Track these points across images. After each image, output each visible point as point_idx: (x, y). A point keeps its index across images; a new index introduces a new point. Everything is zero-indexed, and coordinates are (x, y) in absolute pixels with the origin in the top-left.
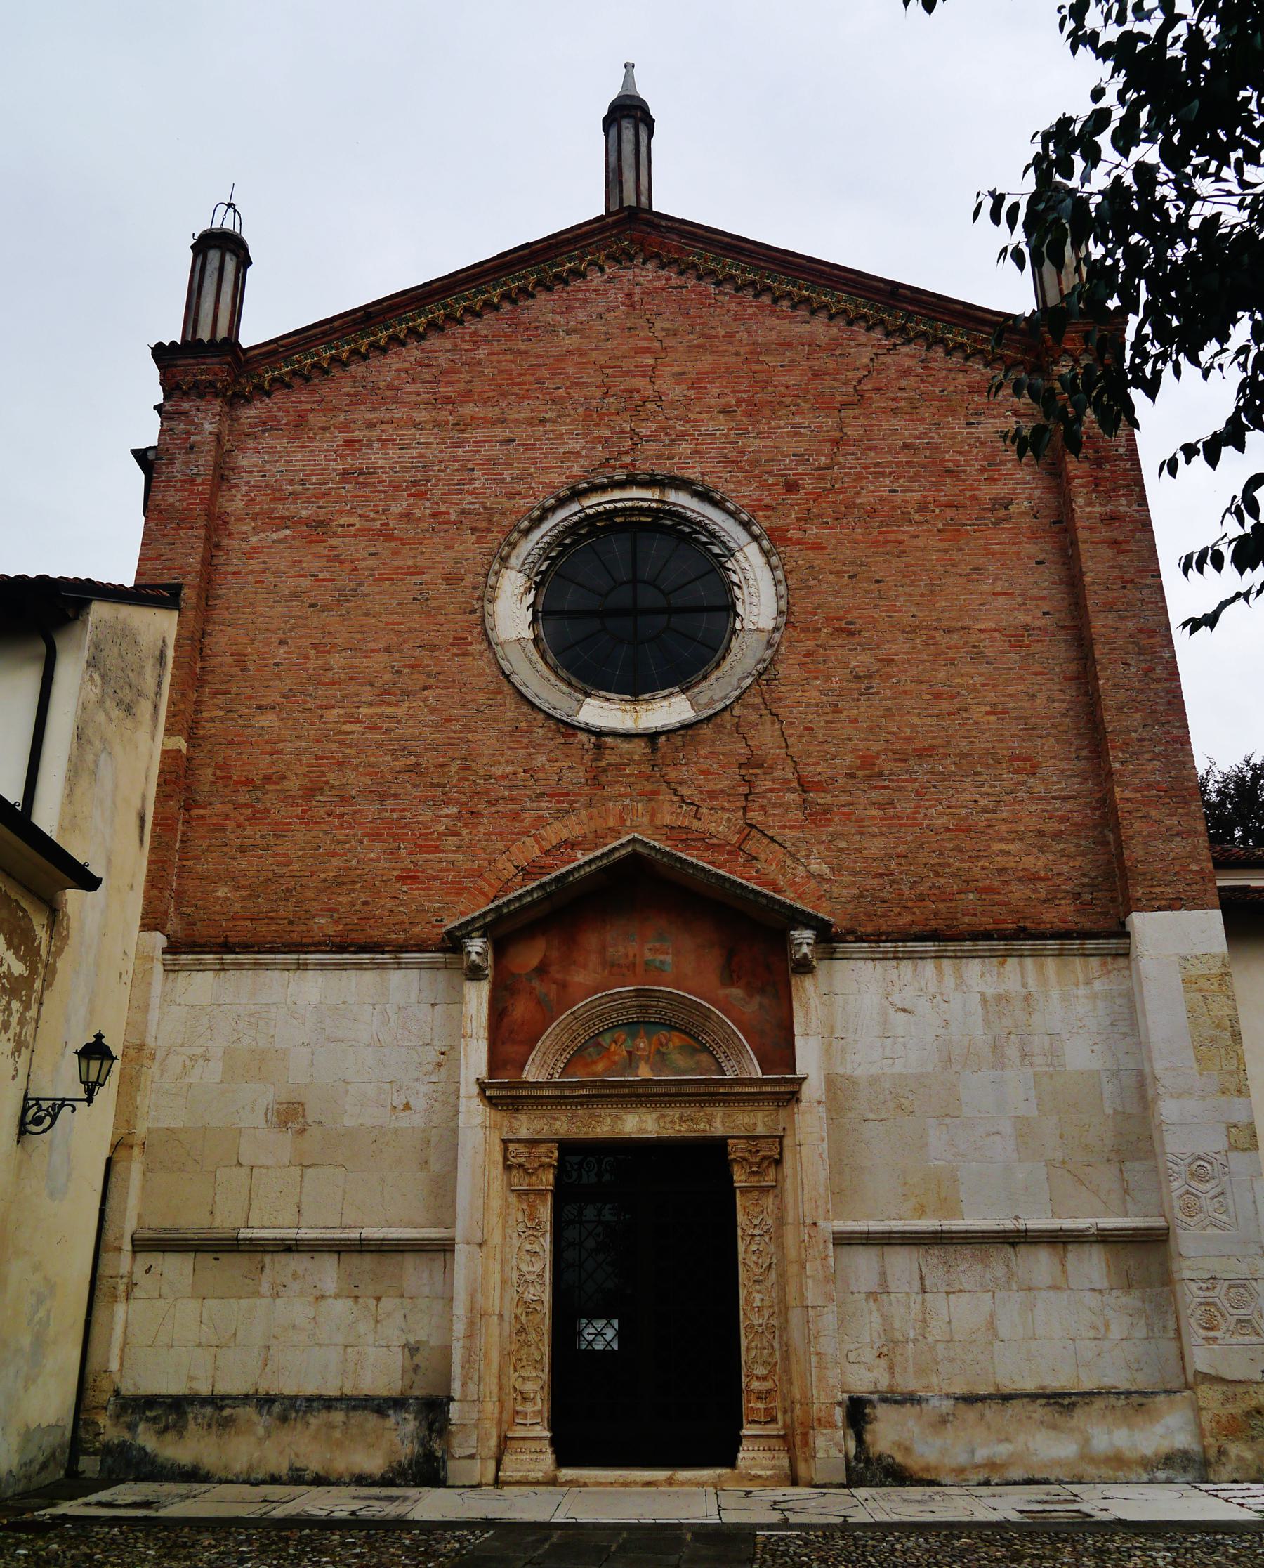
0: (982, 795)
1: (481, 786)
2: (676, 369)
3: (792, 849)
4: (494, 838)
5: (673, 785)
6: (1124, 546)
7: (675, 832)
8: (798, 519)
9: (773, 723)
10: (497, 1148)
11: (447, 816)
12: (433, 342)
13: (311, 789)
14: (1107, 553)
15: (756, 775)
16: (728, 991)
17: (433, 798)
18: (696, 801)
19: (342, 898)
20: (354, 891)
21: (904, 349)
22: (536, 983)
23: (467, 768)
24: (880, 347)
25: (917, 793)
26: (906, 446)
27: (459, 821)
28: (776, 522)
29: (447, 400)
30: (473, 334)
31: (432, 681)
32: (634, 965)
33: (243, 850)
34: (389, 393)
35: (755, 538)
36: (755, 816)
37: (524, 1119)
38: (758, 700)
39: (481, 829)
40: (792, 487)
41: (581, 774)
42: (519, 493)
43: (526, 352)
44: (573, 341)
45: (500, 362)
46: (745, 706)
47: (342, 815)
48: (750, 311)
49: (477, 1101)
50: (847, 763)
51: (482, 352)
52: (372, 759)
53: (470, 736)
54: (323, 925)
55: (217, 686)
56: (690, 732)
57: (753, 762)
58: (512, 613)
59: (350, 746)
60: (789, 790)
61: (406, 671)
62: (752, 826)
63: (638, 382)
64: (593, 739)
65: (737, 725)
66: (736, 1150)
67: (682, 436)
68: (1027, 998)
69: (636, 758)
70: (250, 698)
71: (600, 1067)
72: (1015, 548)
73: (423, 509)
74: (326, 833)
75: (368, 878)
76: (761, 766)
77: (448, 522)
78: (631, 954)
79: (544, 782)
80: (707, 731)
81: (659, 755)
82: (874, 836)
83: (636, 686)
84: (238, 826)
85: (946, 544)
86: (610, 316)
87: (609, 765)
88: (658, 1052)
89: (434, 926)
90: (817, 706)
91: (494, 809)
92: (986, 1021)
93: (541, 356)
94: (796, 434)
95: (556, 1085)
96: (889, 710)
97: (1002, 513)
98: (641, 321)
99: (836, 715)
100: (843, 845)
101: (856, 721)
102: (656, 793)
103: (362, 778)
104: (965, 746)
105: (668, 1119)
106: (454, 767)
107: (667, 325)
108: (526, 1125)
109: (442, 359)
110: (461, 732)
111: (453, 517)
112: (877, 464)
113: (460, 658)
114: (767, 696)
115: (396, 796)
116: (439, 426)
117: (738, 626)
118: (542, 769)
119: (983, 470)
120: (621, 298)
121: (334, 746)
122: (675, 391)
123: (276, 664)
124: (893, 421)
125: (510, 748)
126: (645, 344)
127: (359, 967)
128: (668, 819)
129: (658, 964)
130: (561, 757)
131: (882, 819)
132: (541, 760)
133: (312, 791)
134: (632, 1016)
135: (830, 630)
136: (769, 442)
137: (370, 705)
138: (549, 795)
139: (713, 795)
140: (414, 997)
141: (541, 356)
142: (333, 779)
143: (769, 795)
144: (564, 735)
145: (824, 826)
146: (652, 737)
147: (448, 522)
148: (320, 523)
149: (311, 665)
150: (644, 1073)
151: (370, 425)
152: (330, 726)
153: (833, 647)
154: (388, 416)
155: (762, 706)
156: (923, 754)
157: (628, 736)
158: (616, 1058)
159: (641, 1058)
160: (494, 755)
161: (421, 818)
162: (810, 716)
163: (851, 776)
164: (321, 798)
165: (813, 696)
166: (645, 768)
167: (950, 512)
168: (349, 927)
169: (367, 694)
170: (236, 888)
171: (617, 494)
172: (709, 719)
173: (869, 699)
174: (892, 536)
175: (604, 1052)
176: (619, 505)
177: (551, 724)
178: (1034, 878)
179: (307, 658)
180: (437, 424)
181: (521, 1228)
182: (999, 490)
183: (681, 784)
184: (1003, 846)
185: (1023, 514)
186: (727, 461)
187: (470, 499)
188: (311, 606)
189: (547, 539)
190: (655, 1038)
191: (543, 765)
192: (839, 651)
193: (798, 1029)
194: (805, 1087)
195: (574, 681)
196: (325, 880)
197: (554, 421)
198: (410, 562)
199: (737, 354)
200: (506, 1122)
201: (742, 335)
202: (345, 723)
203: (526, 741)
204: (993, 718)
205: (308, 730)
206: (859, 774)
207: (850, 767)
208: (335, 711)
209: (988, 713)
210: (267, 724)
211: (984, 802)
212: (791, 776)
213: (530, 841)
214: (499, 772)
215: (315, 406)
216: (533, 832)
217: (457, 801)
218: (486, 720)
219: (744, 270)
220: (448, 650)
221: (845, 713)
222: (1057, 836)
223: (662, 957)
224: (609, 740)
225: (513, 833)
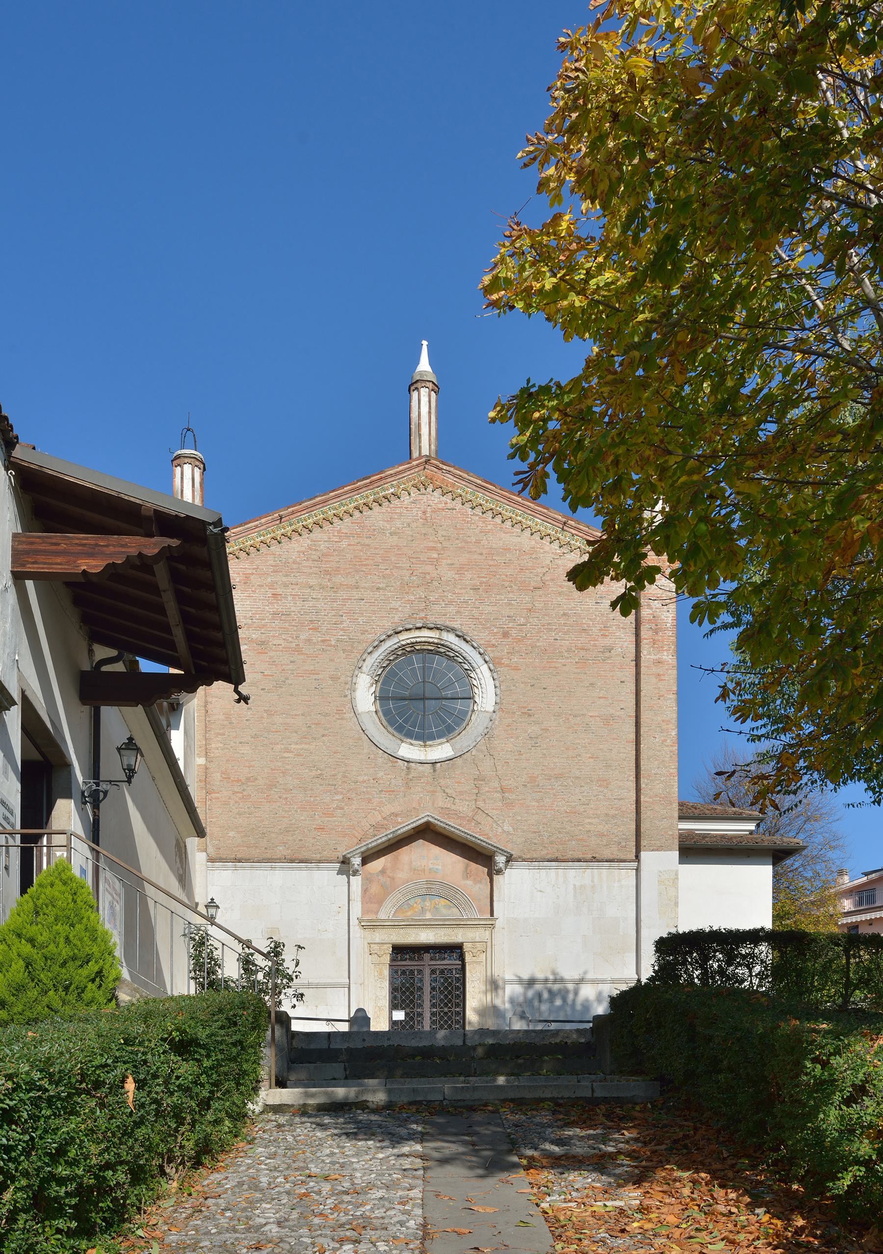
0: (583, 796)
1: (353, 786)
2: (449, 562)
6: (662, 677)
7: (445, 810)
8: (508, 653)
12: (317, 534)
14: (654, 680)
16: (465, 882)
17: (330, 791)
21: (568, 556)
22: (380, 877)
23: (345, 777)
24: (556, 554)
25: (554, 795)
26: (564, 614)
28: (497, 654)
29: (327, 572)
30: (339, 531)
31: (326, 732)
33: (239, 814)
34: (295, 566)
35: (486, 662)
36: (480, 804)
38: (484, 748)
40: (506, 635)
42: (367, 631)
43: (368, 545)
44: (394, 540)
45: (354, 550)
46: (478, 751)
48: (489, 527)
51: (344, 543)
54: (281, 851)
55: (218, 731)
57: (480, 778)
58: (365, 697)
63: (429, 568)
65: (474, 760)
66: (467, 947)
67: (451, 602)
68: (593, 887)
70: (235, 737)
71: (409, 913)
72: (611, 674)
73: (317, 637)
77: (330, 646)
81: (437, 773)
83: (424, 737)
84: (236, 802)
85: (579, 670)
86: (414, 525)
92: (575, 896)
93: (376, 548)
94: (510, 604)
95: (392, 920)
97: (607, 654)
98: (431, 531)
100: (519, 818)
102: (434, 792)
104: (578, 773)
106: (339, 776)
107: (444, 533)
109: (323, 546)
111: (333, 643)
112: (549, 624)
116: (323, 588)
117: (475, 708)
119: (601, 630)
120: (420, 514)
121: (280, 764)
122: (449, 575)
124: (559, 599)
126: (432, 544)
127: (300, 869)
128: (441, 804)
132: (381, 774)
133: (270, 787)
134: (424, 892)
136: (495, 608)
139: (461, 793)
141: (376, 548)
144: (392, 762)
147: (330, 646)
148: (263, 643)
150: (428, 916)
151: (285, 586)
153: (521, 722)
154: (294, 581)
156: (558, 777)
167: (582, 653)
170: (238, 832)
171: (417, 633)
174: (553, 665)
175: (411, 907)
176: (418, 640)
178: (603, 835)
179: (262, 717)
180: (322, 587)
181: (376, 978)
182: (607, 642)
184: (590, 821)
185: (617, 655)
186: (473, 618)
187: (341, 633)
188: (263, 689)
189: (381, 657)
195: (395, 733)
197: (385, 589)
198: (312, 668)
199: (481, 554)
201: (484, 542)
204: (592, 760)
208: (279, 746)
210: (245, 752)
211: (583, 800)
213: (376, 813)
215: (254, 571)
219: (487, 501)
222: (614, 817)
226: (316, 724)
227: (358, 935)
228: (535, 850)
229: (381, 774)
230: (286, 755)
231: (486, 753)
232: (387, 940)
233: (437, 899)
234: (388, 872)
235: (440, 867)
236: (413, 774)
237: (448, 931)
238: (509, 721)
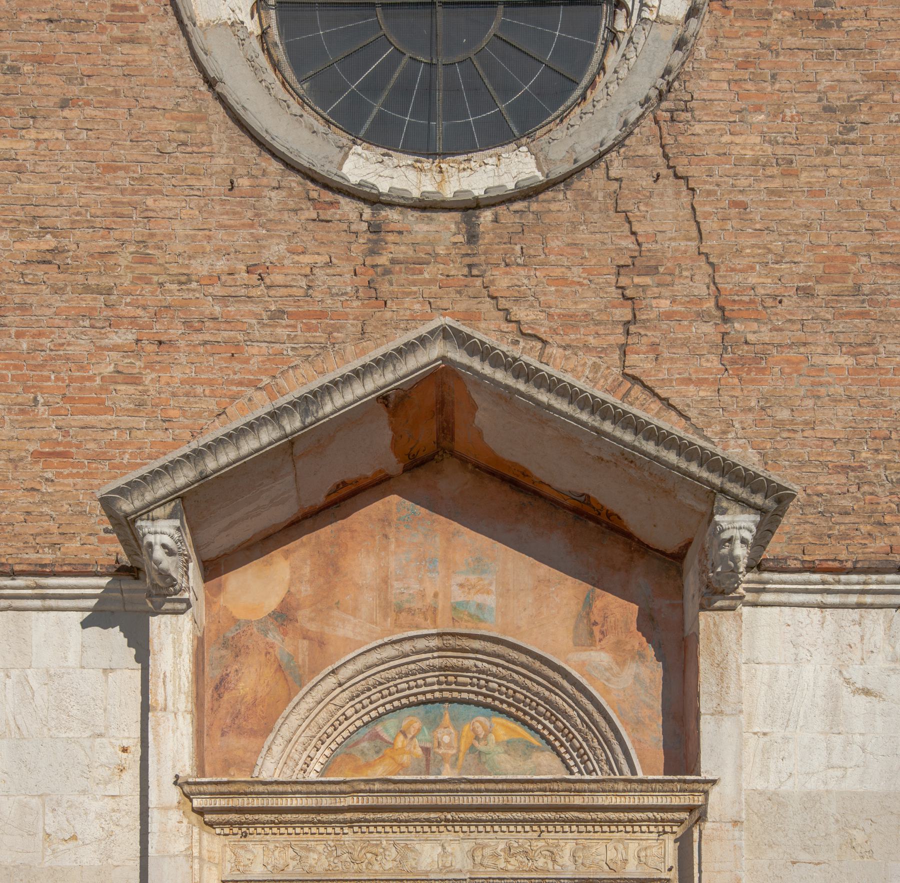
4: (199, 390)
5: (503, 303)
9: (678, 193)
11: (115, 348)
15: (645, 288)
18: (542, 332)
31: (75, 90)
36: (640, 363)
38: (654, 150)
41: (348, 277)
50: (801, 269)
57: (640, 263)
60: (701, 316)
61: (27, 68)
62: (635, 379)
64: (367, 212)
69: (441, 250)
76: (652, 271)
79: (283, 291)
87: (393, 261)
90: (755, 162)
91: (198, 338)
96: (879, 172)
99: (787, 181)
100: (785, 414)
101: (822, 192)
106: (124, 258)
110: (135, 192)
113: (126, 48)
114: (669, 140)
115: (23, 307)
125: (222, 226)
130: (311, 246)
131: (854, 372)
132: (276, 249)
135: (788, 14)
138: (290, 315)
139: (570, 321)
146: (469, 207)
155: (661, 161)
157: (427, 206)
160: (193, 238)
161: (70, 350)
162: (743, 182)
163: (806, 293)
165: (750, 144)
166: (457, 270)
172: (566, 179)
173: (847, 153)
177: (294, 180)
183: (517, 300)
191: (281, 259)
203: (250, 214)
206: (821, 289)
207: (806, 277)
212: (704, 291)
214: (204, 271)
216: (266, 380)
218: (177, 171)
220: (102, 30)
221: (804, 177)
226: (38, 60)
228: (844, 536)
231: (664, 171)
236: (395, 249)
238: (751, 44)
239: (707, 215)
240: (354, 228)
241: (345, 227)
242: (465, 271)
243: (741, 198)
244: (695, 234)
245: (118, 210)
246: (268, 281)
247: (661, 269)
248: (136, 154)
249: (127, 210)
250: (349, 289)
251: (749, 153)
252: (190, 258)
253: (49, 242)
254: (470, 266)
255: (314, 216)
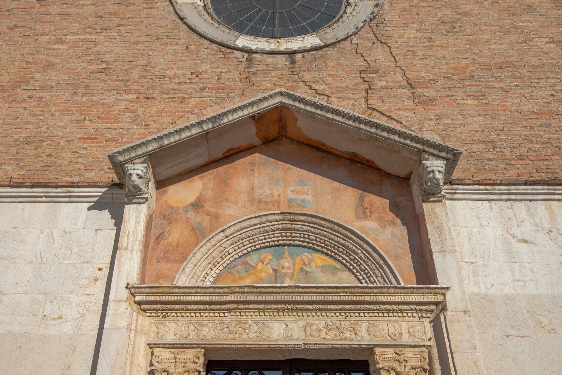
3: (408, 124)
4: (164, 114)
5: (308, 83)
9: (383, 48)
10: (142, 352)
11: (127, 100)
13: (19, 82)
15: (373, 78)
16: (362, 223)
17: (117, 89)
18: (327, 93)
19: (28, 152)
20: (40, 147)
22: (191, 214)
27: (137, 103)
32: (279, 202)
36: (374, 103)
37: (172, 325)
38: (371, 35)
39: (154, 109)
41: (237, 76)
47: (41, 98)
49: (124, 305)
52: (72, 65)
53: (151, 53)
56: (320, 52)
59: (56, 57)
60: (401, 87)
62: (373, 109)
64: (246, 55)
69: (279, 67)
74: (25, 109)
75: (55, 139)
76: (377, 72)
78: (276, 194)
80: (332, 52)
81: (297, 65)
82: (473, 116)
87: (257, 70)
88: (302, 270)
89: (106, 173)
90: (416, 38)
91: (165, 96)
95: (205, 290)
99: (430, 44)
103: (62, 76)
105: (314, 328)
108: (174, 329)
113: (148, 10)
114: (376, 32)
115: (87, 87)
118: (206, 72)
121: (43, 57)
123: (7, 11)
125: (181, 60)
127: (34, 200)
129: (299, 202)
130: (220, 66)
132: (204, 67)
134: (278, 237)
137: (76, 34)
138: (209, 88)
139: (340, 89)
140: (80, 225)
142: (37, 76)
143: (384, 90)
145: (430, 109)
146: (291, 54)
149: (34, 13)
152: (41, 45)
155: (374, 38)
158: (263, 275)
159: (285, 275)
160: (168, 64)
161: (105, 101)
162: (411, 44)
164: (26, 88)
166: (287, 73)
168: (32, 172)
169: (75, 27)
172: (334, 44)
173: (455, 35)
175: (250, 268)
177: (214, 46)
183: (314, 82)
190: (298, 259)
191: (207, 70)
192: (428, 8)
193: (435, 247)
194: (449, 294)
196: (17, 140)
200: (153, 328)
202: (54, 44)
205: (25, 48)
206: (455, 77)
208: (47, 37)
209: (547, 43)
212: (401, 79)
214: (172, 74)
217: (137, 91)
221: (438, 42)
223: (303, 197)
224: (258, 56)
225: (180, 112)
227: (124, 322)
229: (204, 67)
230: (56, 46)
232: (193, 338)
233: (306, 255)
234: (208, 206)
235: (309, 198)
237: (336, 319)
239: (397, 55)
240: (239, 60)
241: (236, 60)
242: (291, 73)
243: (411, 49)
244: (393, 60)
245: (136, 56)
246: (200, 77)
247: (380, 72)
248: (147, 39)
249: (139, 56)
250: (237, 79)
251: (412, 36)
252: (166, 70)
253: (104, 65)
254: (292, 72)
255: (223, 56)
